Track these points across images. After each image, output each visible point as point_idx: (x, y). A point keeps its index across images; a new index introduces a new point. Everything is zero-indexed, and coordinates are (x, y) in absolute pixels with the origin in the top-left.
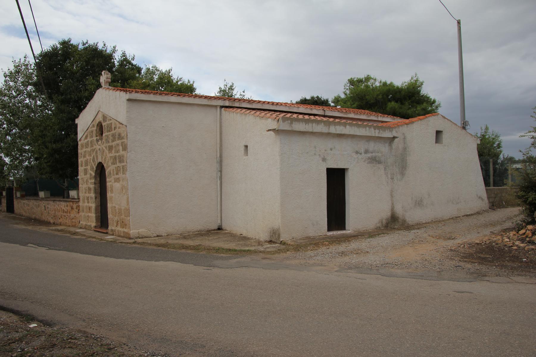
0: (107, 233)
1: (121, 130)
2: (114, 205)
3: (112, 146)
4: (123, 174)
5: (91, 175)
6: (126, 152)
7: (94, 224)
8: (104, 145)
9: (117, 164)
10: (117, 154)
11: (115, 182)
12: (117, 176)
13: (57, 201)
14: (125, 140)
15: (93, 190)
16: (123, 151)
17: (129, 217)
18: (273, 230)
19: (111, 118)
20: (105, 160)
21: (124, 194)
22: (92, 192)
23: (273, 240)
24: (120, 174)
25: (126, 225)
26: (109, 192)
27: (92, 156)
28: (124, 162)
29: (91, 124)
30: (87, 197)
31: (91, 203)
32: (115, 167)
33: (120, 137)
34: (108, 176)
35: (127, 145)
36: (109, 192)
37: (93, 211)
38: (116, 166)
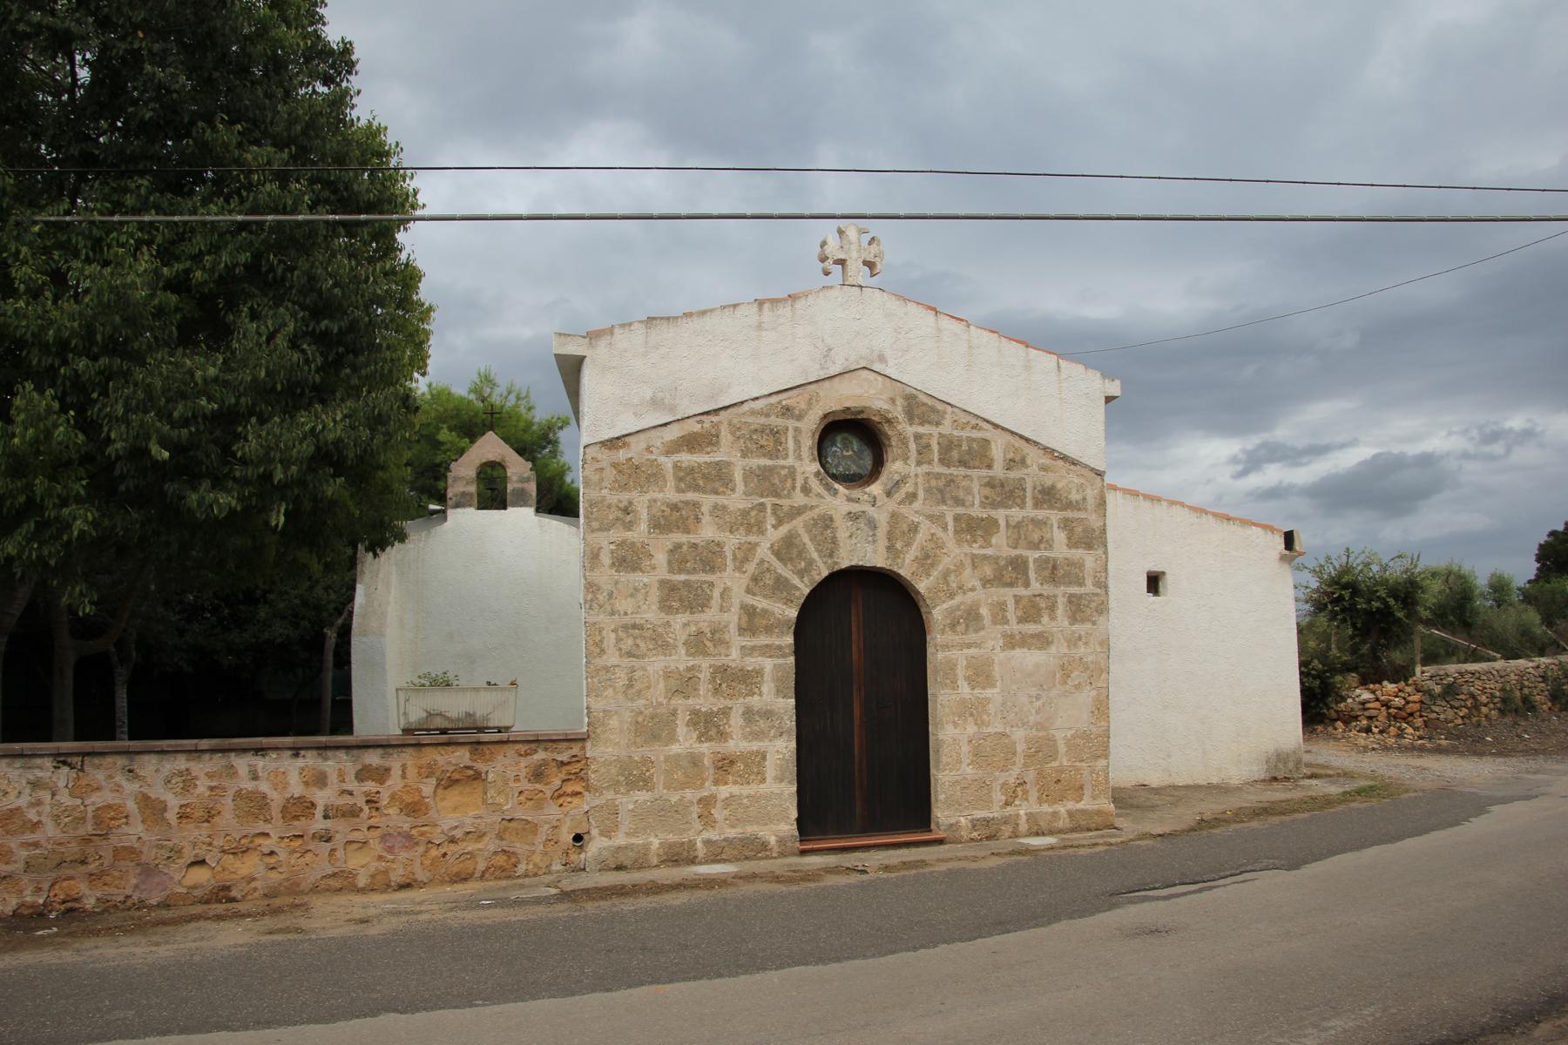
0: (940, 842)
1: (1065, 480)
2: (997, 727)
4: (1073, 619)
5: (750, 612)
6: (1100, 552)
8: (917, 505)
9: (1027, 585)
10: (1032, 555)
11: (1013, 648)
12: (1032, 628)
14: (1094, 520)
16: (1072, 544)
17: (1106, 757)
18: (1278, 755)
19: (974, 421)
22: (768, 687)
24: (1053, 618)
25: (1081, 788)
27: (774, 535)
28: (1081, 584)
33: (1048, 496)
35: (1104, 531)
37: (770, 770)
38: (1021, 591)
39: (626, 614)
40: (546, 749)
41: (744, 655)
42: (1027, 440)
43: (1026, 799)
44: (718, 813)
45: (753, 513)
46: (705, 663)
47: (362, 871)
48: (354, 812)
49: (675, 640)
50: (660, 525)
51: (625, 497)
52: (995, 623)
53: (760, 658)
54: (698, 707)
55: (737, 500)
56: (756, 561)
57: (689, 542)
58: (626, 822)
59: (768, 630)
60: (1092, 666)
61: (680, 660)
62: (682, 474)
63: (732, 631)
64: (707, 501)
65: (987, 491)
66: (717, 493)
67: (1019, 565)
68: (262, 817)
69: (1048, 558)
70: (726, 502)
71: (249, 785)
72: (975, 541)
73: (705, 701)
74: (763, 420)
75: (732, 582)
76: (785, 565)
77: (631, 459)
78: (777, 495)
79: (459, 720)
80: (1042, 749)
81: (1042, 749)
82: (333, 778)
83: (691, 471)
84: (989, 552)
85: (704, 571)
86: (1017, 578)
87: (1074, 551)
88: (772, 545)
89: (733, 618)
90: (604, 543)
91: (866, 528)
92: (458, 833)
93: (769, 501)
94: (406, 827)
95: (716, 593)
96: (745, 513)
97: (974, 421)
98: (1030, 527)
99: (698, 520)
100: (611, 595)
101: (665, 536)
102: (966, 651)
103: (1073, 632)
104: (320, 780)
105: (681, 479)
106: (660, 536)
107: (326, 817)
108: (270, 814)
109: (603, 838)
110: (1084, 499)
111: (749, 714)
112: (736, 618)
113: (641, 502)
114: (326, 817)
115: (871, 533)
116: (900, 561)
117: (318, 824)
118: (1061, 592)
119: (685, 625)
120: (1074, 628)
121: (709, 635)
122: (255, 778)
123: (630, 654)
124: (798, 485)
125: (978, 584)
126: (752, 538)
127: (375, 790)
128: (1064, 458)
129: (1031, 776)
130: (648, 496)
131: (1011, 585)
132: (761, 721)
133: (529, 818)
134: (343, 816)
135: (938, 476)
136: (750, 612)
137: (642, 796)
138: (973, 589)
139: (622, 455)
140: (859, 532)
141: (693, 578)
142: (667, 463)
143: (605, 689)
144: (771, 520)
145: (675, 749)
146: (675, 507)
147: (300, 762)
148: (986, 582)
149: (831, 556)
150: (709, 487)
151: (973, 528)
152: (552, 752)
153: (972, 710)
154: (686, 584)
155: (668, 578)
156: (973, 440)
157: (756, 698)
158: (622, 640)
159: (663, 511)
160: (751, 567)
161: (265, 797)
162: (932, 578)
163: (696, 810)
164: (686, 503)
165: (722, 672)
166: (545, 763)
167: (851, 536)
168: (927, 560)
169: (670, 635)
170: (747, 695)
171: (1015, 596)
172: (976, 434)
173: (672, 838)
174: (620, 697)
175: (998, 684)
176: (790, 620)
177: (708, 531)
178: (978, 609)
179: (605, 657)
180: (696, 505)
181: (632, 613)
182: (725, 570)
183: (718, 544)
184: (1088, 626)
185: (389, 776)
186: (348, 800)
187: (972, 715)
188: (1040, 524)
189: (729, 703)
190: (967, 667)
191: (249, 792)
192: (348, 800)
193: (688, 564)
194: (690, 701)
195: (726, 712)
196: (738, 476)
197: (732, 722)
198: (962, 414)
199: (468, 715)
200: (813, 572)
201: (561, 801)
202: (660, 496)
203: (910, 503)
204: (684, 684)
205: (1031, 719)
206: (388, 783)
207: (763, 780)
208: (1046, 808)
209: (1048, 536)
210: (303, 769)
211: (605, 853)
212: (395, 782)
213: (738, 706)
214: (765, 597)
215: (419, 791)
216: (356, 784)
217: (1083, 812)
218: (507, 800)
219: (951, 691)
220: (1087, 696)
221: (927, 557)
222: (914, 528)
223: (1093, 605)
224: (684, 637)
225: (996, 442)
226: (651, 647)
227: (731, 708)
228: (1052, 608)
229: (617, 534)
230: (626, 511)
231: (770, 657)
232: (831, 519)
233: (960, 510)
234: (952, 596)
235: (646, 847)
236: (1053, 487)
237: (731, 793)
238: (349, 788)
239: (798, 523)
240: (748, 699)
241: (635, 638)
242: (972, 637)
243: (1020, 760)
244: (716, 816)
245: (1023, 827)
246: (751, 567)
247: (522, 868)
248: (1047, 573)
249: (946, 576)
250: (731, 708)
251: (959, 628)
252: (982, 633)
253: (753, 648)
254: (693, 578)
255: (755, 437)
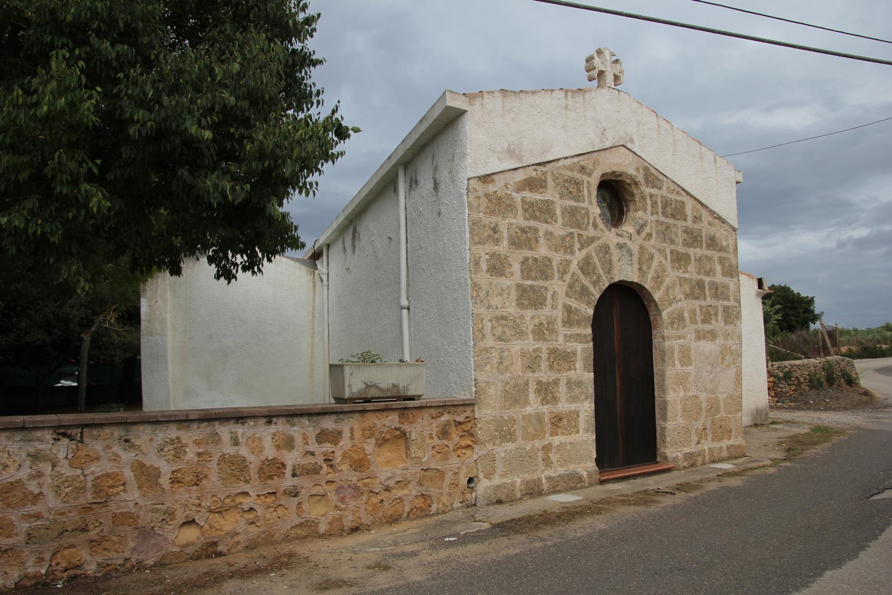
0: (669, 470)
3: (688, 256)
4: (726, 322)
5: (568, 309)
6: (736, 280)
7: (587, 466)
8: (652, 241)
9: (705, 299)
10: (707, 279)
11: (699, 340)
12: (708, 327)
13: (217, 423)
15: (585, 359)
18: (757, 411)
20: (656, 282)
21: (728, 366)
22: (579, 364)
23: (758, 422)
24: (717, 321)
26: (677, 362)
27: (579, 255)
28: (729, 300)
29: (566, 158)
30: (539, 383)
31: (574, 399)
32: (701, 307)
33: (712, 243)
34: (672, 323)
36: (677, 362)
37: (582, 425)
39: (497, 308)
40: (449, 413)
41: (566, 341)
42: (702, 204)
43: (707, 439)
44: (554, 457)
45: (568, 239)
46: (544, 346)
47: (322, 519)
48: (315, 470)
49: (527, 328)
50: (516, 243)
51: (493, 219)
52: (691, 323)
53: (574, 344)
54: (541, 379)
55: (558, 229)
56: (570, 273)
57: (533, 257)
58: (500, 467)
59: (579, 323)
60: (734, 352)
61: (530, 344)
62: (526, 207)
63: (559, 323)
64: (542, 228)
65: (685, 235)
66: (547, 223)
67: (700, 284)
68: (242, 478)
69: (714, 281)
70: (552, 230)
71: (230, 450)
72: (680, 268)
73: (544, 374)
74: (570, 174)
75: (557, 286)
76: (586, 277)
77: (496, 192)
78: (580, 228)
79: (388, 390)
80: (713, 407)
81: (713, 407)
82: (299, 441)
83: (531, 205)
84: (687, 276)
85: (542, 279)
86: (700, 294)
87: (724, 278)
88: (579, 262)
89: (559, 314)
90: (483, 254)
91: (627, 255)
92: (391, 483)
93: (576, 231)
94: (354, 479)
95: (549, 296)
96: (563, 238)
97: (678, 189)
98: (705, 261)
99: (537, 241)
100: (487, 293)
101: (519, 251)
102: (678, 341)
103: (726, 331)
104: (289, 443)
105: (526, 210)
106: (516, 251)
107: (294, 475)
108: (249, 475)
109: (486, 480)
110: (728, 245)
111: (569, 382)
112: (561, 313)
113: (503, 224)
114: (294, 475)
115: (630, 259)
116: (645, 278)
117: (288, 482)
118: (721, 303)
119: (533, 318)
120: (727, 327)
121: (546, 326)
122: (236, 443)
123: (500, 339)
124: (591, 221)
125: (682, 296)
126: (568, 257)
127: (330, 450)
128: (719, 218)
129: (708, 425)
130: (507, 221)
131: (697, 298)
132: (576, 389)
133: (439, 468)
134: (308, 473)
135: (662, 223)
136: (568, 309)
137: (510, 446)
138: (680, 300)
139: (491, 188)
140: (623, 257)
141: (536, 283)
142: (517, 197)
143: (486, 365)
144: (577, 246)
145: (529, 410)
146: (523, 231)
147: (273, 429)
148: (687, 296)
149: (609, 273)
150: (542, 218)
151: (680, 259)
152: (453, 414)
153: (682, 380)
154: (532, 287)
155: (521, 282)
156: (677, 201)
157: (573, 372)
158: (495, 328)
159: (517, 233)
160: (568, 277)
161: (244, 460)
162: (661, 291)
163: (541, 454)
164: (530, 228)
165: (553, 352)
166: (448, 423)
167: (619, 260)
168: (658, 279)
169: (524, 325)
170: (568, 370)
171: (700, 306)
172: (679, 198)
173: (528, 477)
174: (495, 371)
175: (694, 364)
176: (589, 317)
177: (543, 250)
178: (683, 313)
179: (485, 340)
180: (535, 230)
181: (501, 308)
182: (553, 279)
183: (549, 260)
184: (733, 326)
185: (341, 438)
186: (310, 459)
187: (682, 384)
188: (710, 259)
189: (558, 376)
190: (679, 352)
191: (231, 457)
192: (310, 459)
193: (533, 273)
194: (536, 375)
195: (556, 382)
196: (558, 212)
197: (560, 390)
198: (671, 183)
199: (394, 386)
200: (601, 284)
201: (459, 452)
202: (514, 221)
203: (649, 240)
204: (532, 363)
205: (709, 386)
206: (341, 444)
207: (578, 432)
208: (716, 445)
209: (713, 268)
210: (275, 434)
211: (489, 491)
212: (345, 443)
213: (563, 377)
214: (576, 299)
215: (363, 449)
216: (316, 445)
217: (733, 446)
218: (424, 453)
219: (672, 368)
220: (733, 370)
221: (658, 277)
222: (651, 258)
223: (734, 313)
224: (532, 327)
225: (688, 204)
226: (513, 333)
227: (559, 380)
228: (716, 314)
229: (489, 247)
230: (495, 230)
231: (580, 342)
232: (609, 247)
233: (673, 247)
234: (670, 304)
235: (513, 484)
236: (714, 236)
237: (560, 441)
238: (311, 450)
239: (592, 247)
240: (569, 373)
241: (503, 327)
242: (681, 332)
243: (704, 413)
244: (552, 459)
245: (707, 458)
246: (568, 277)
247: (434, 507)
248: (713, 291)
249: (667, 290)
250: (559, 380)
251: (675, 326)
252: (685, 329)
253: (571, 336)
254: (536, 283)
255: (566, 185)
